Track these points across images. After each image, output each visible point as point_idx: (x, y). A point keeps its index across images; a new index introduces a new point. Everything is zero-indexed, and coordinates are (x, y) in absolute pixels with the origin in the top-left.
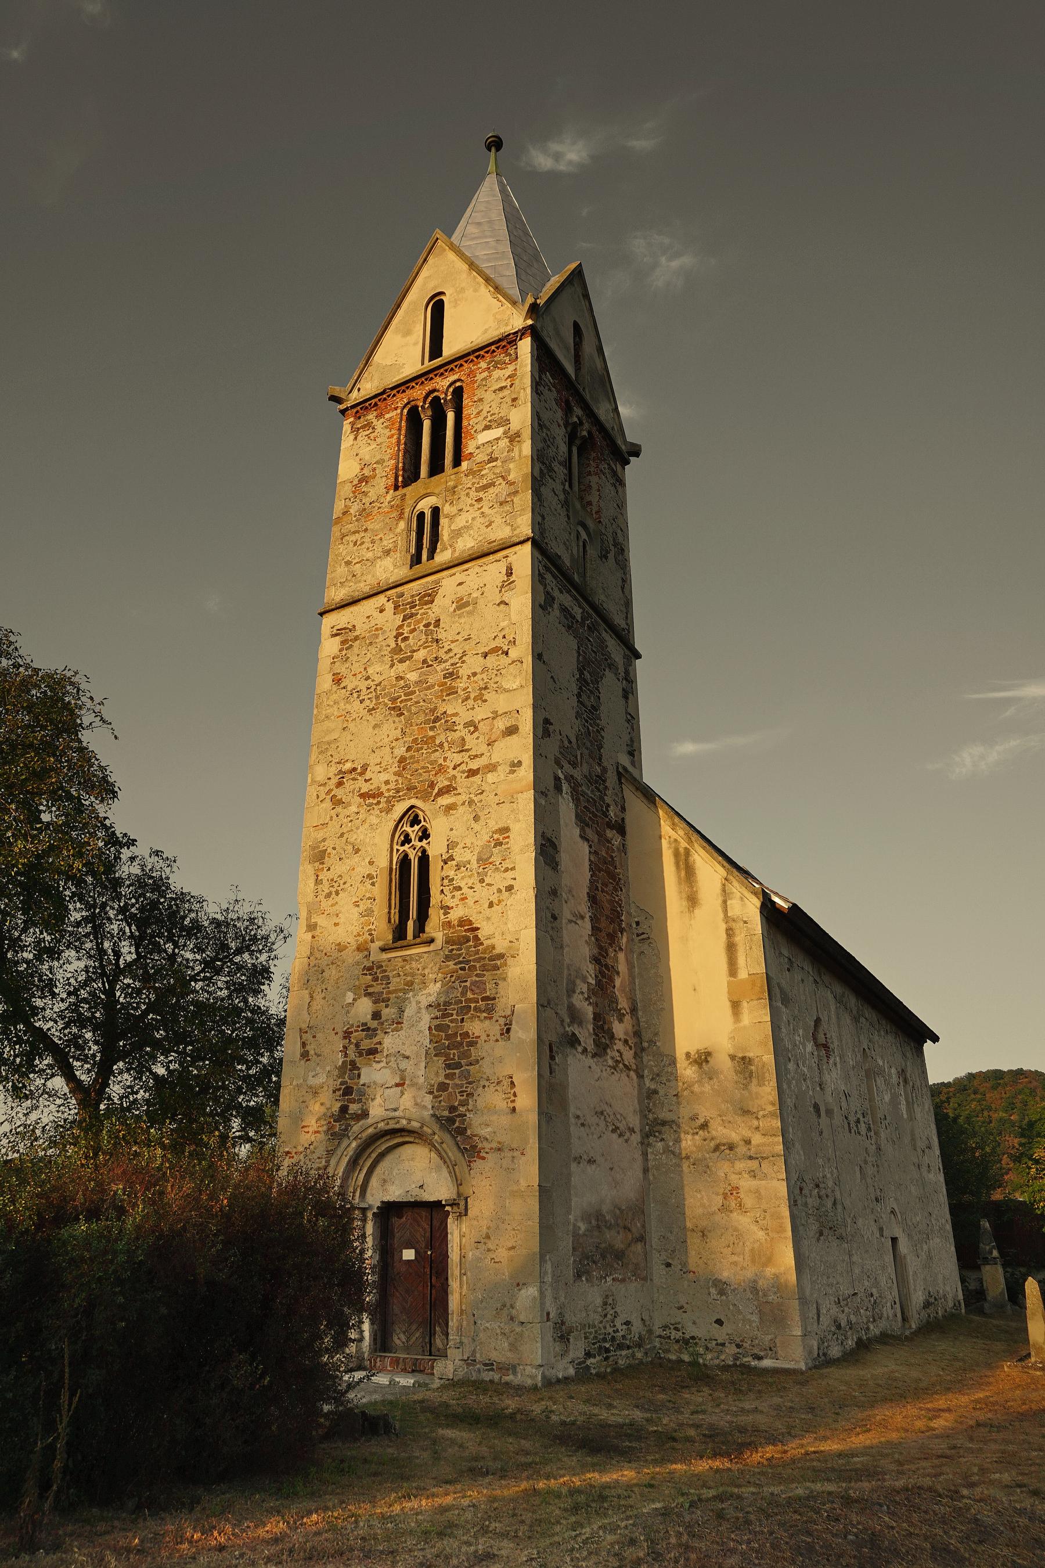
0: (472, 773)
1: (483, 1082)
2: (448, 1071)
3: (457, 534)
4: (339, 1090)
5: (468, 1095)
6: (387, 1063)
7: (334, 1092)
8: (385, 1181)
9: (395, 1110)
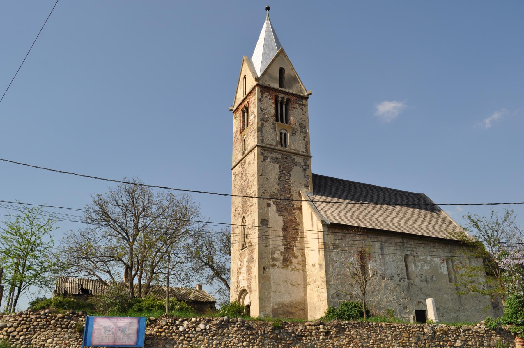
0: (251, 206)
3: (248, 146)
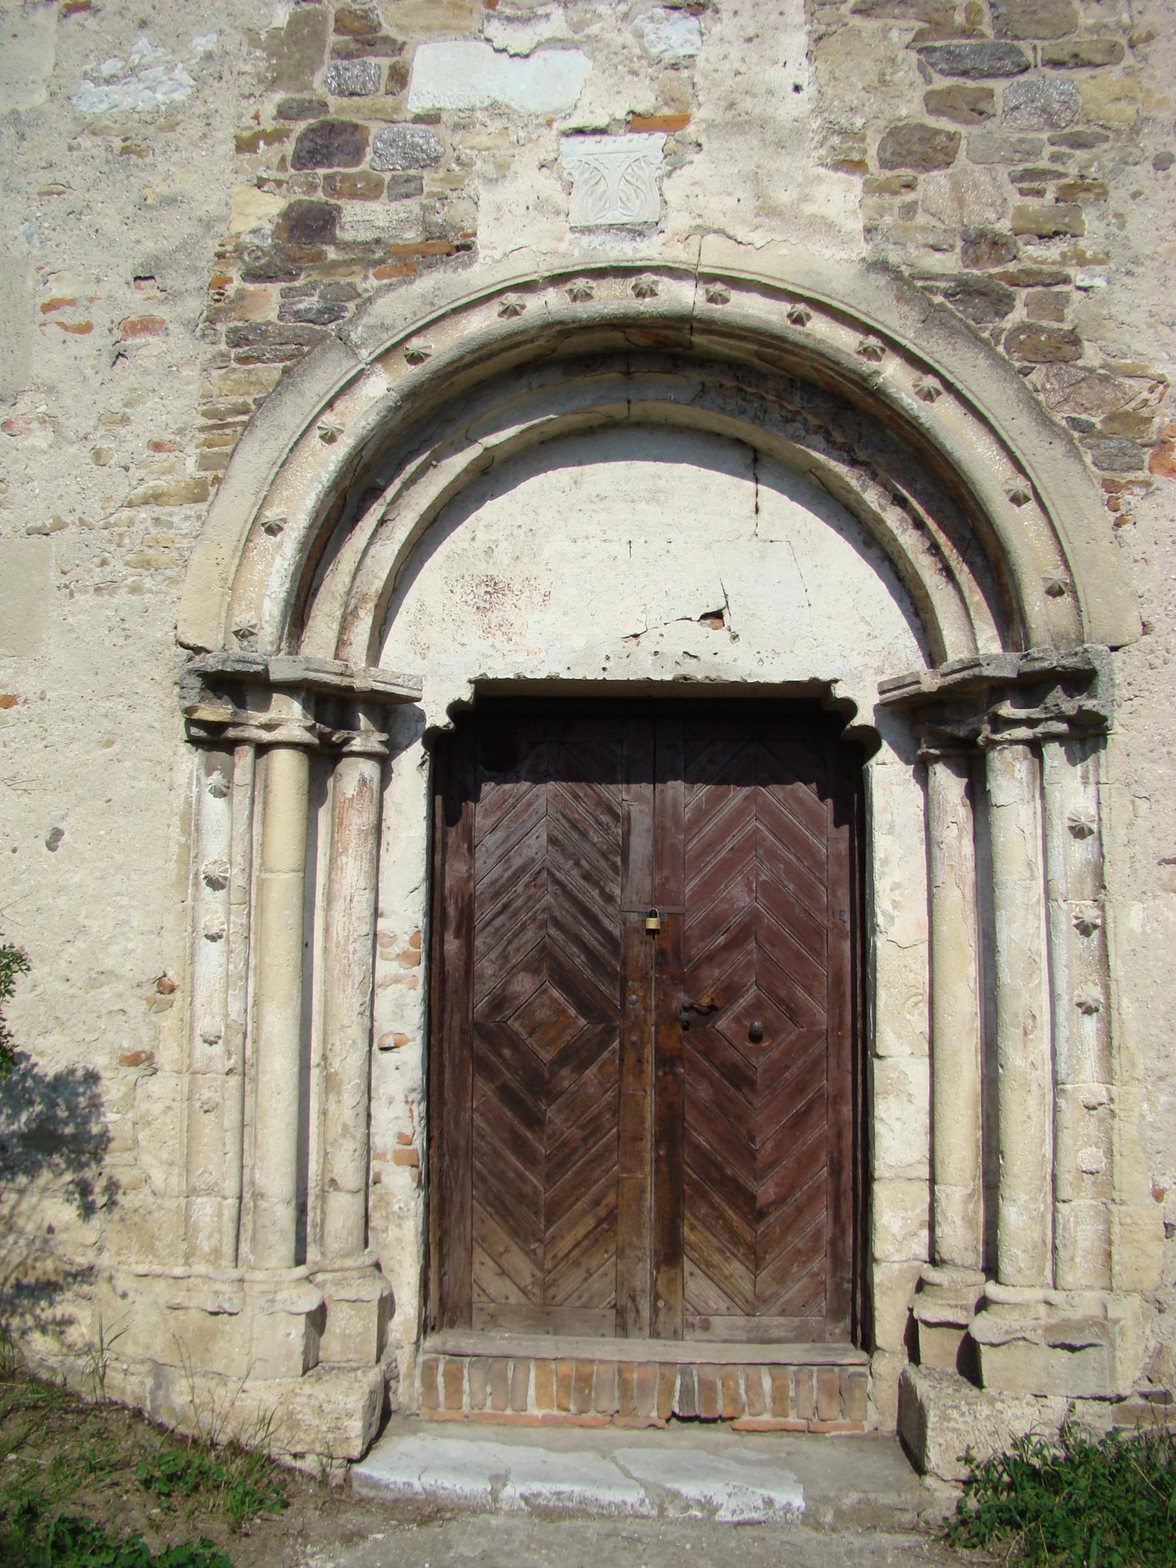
1: (1150, 144)
2: (942, 83)
4: (275, 137)
5: (1067, 194)
6: (577, 27)
7: (245, 146)
8: (494, 587)
9: (636, 232)
